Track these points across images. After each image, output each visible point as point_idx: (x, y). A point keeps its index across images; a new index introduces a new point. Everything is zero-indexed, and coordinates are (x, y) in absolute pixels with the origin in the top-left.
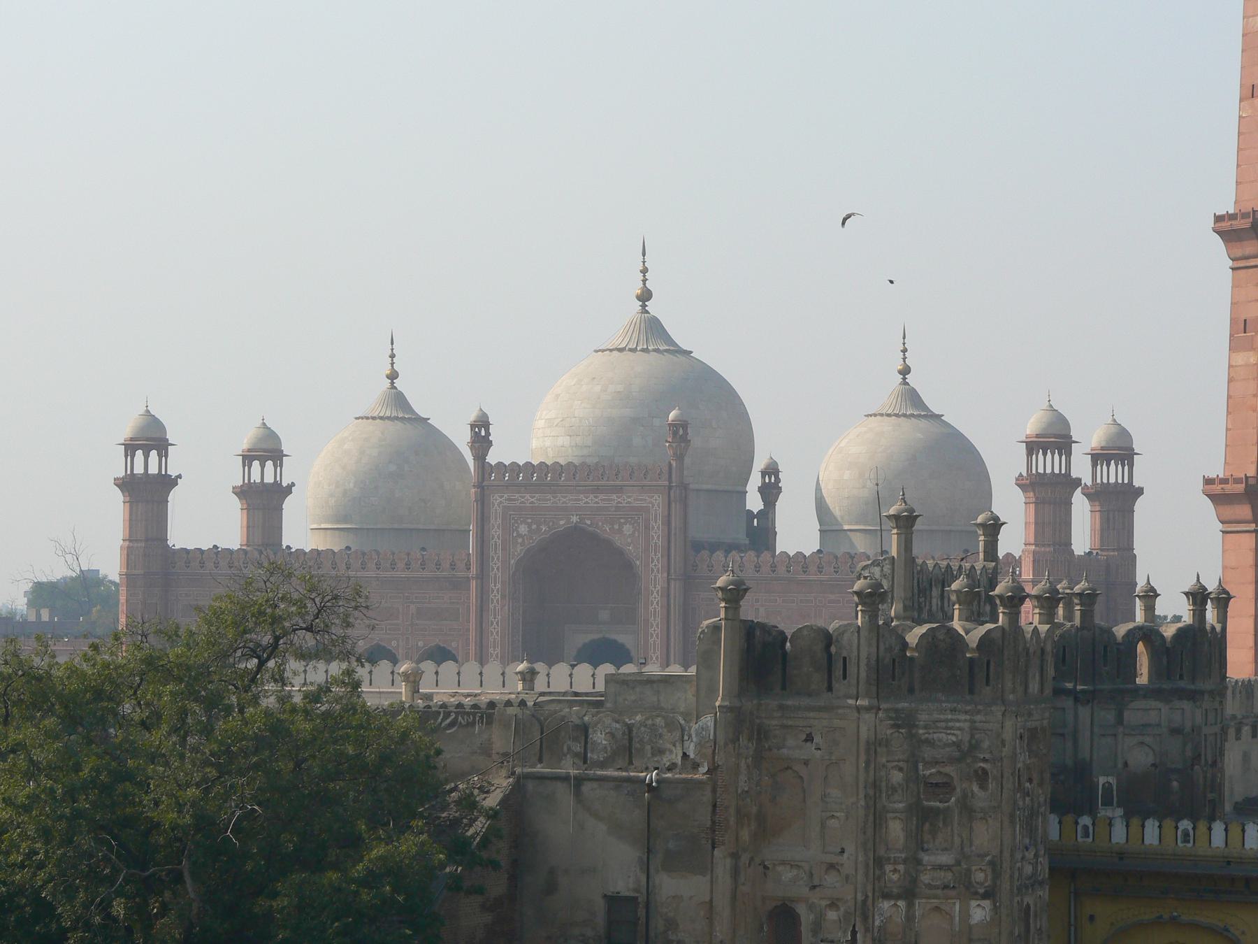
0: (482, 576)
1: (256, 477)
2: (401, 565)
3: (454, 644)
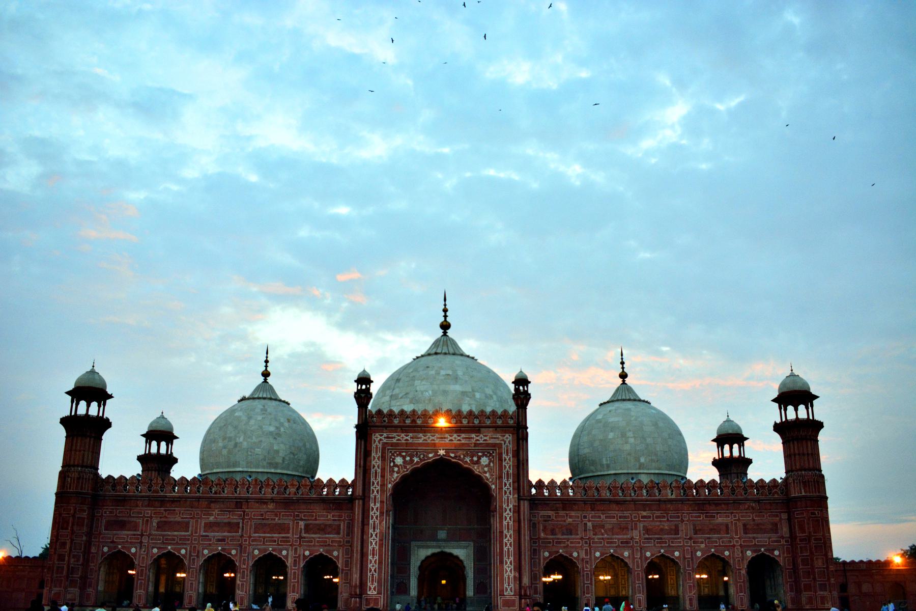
0: (365, 497)
1: (154, 450)
2: (293, 490)
3: (335, 553)
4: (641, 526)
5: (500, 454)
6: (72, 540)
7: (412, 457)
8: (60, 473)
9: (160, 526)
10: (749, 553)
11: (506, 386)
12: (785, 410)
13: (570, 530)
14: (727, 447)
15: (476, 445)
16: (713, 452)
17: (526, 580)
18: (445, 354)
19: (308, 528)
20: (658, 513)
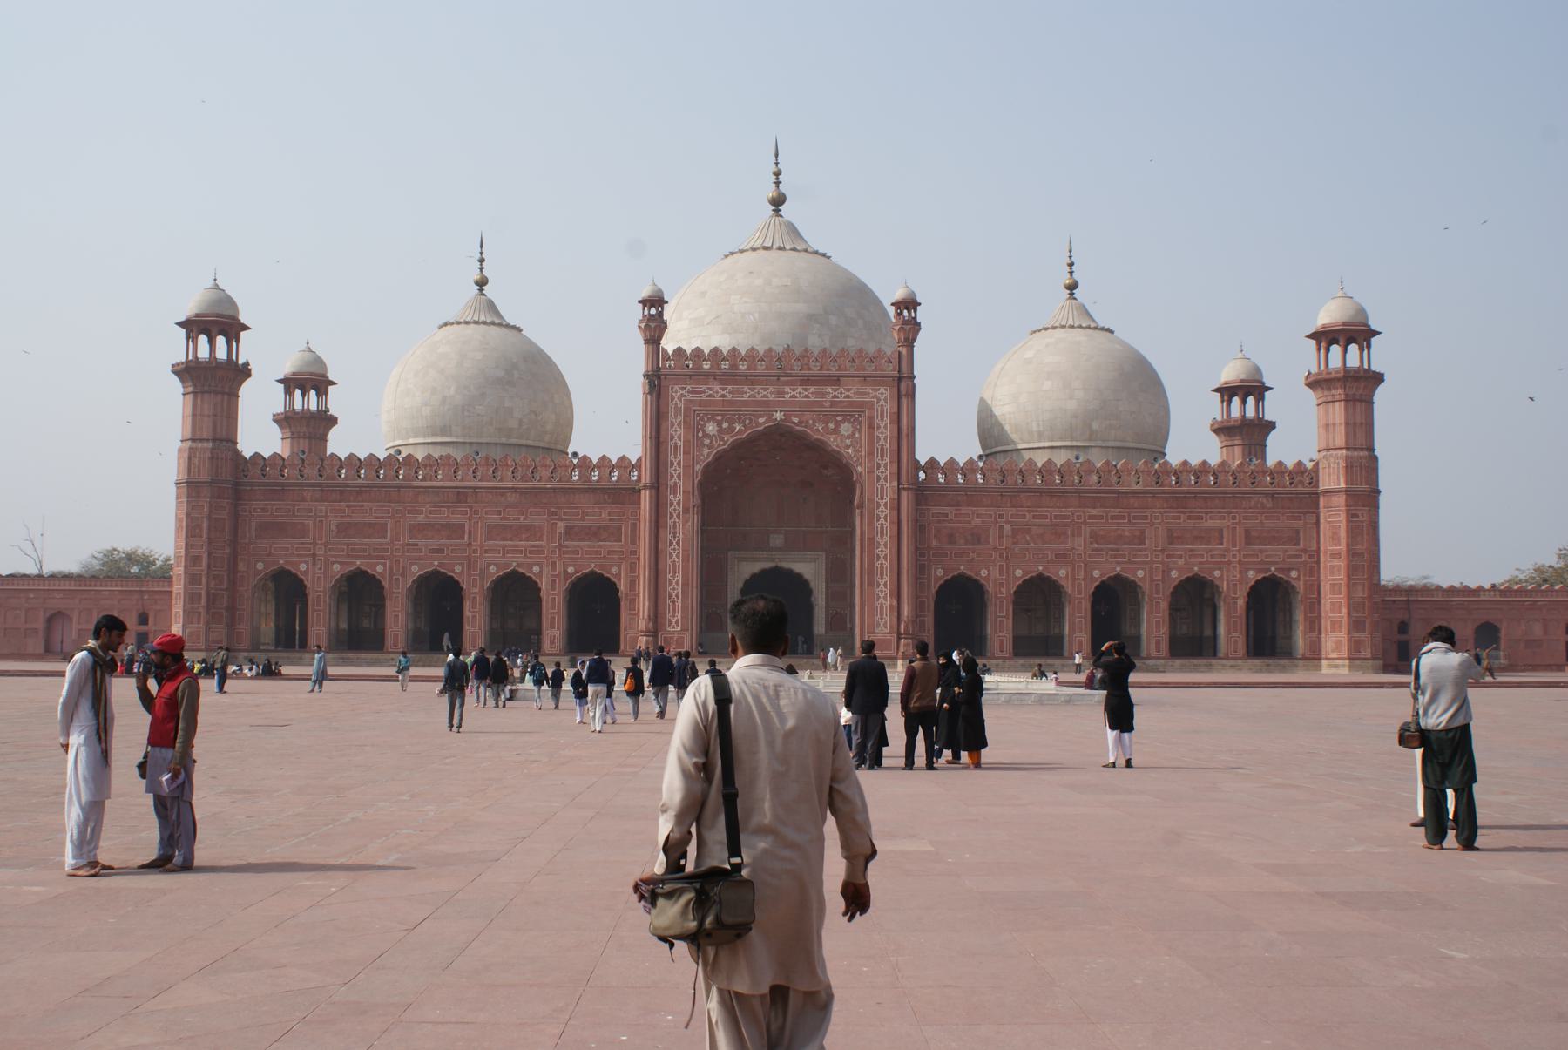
0: (658, 486)
1: (298, 405)
2: (546, 473)
3: (614, 570)
4: (1086, 530)
5: (871, 419)
6: (210, 554)
7: (731, 421)
8: (180, 450)
9: (343, 529)
10: (1251, 573)
11: (877, 302)
12: (1328, 350)
13: (977, 537)
14: (1236, 401)
15: (833, 404)
16: (1213, 409)
17: (906, 611)
18: (780, 248)
19: (570, 532)
20: (1115, 512)
